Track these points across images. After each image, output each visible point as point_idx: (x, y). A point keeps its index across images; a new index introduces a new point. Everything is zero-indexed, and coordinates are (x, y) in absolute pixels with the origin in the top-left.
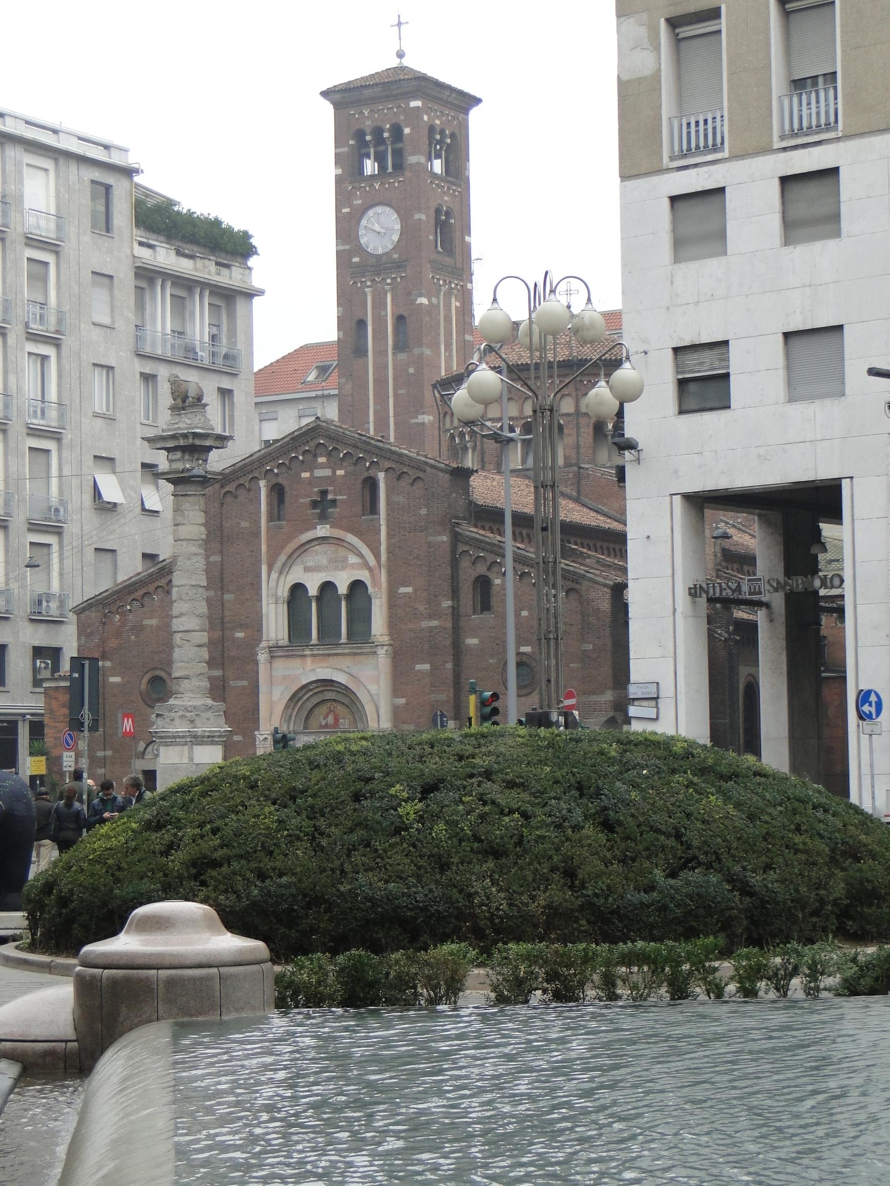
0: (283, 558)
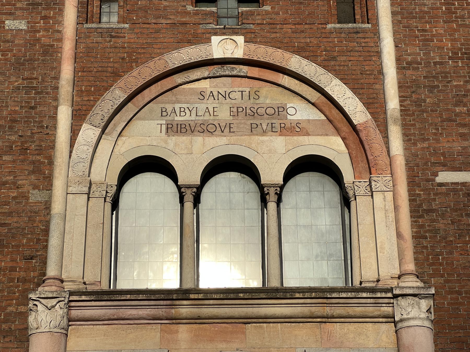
0: (117, 94)
